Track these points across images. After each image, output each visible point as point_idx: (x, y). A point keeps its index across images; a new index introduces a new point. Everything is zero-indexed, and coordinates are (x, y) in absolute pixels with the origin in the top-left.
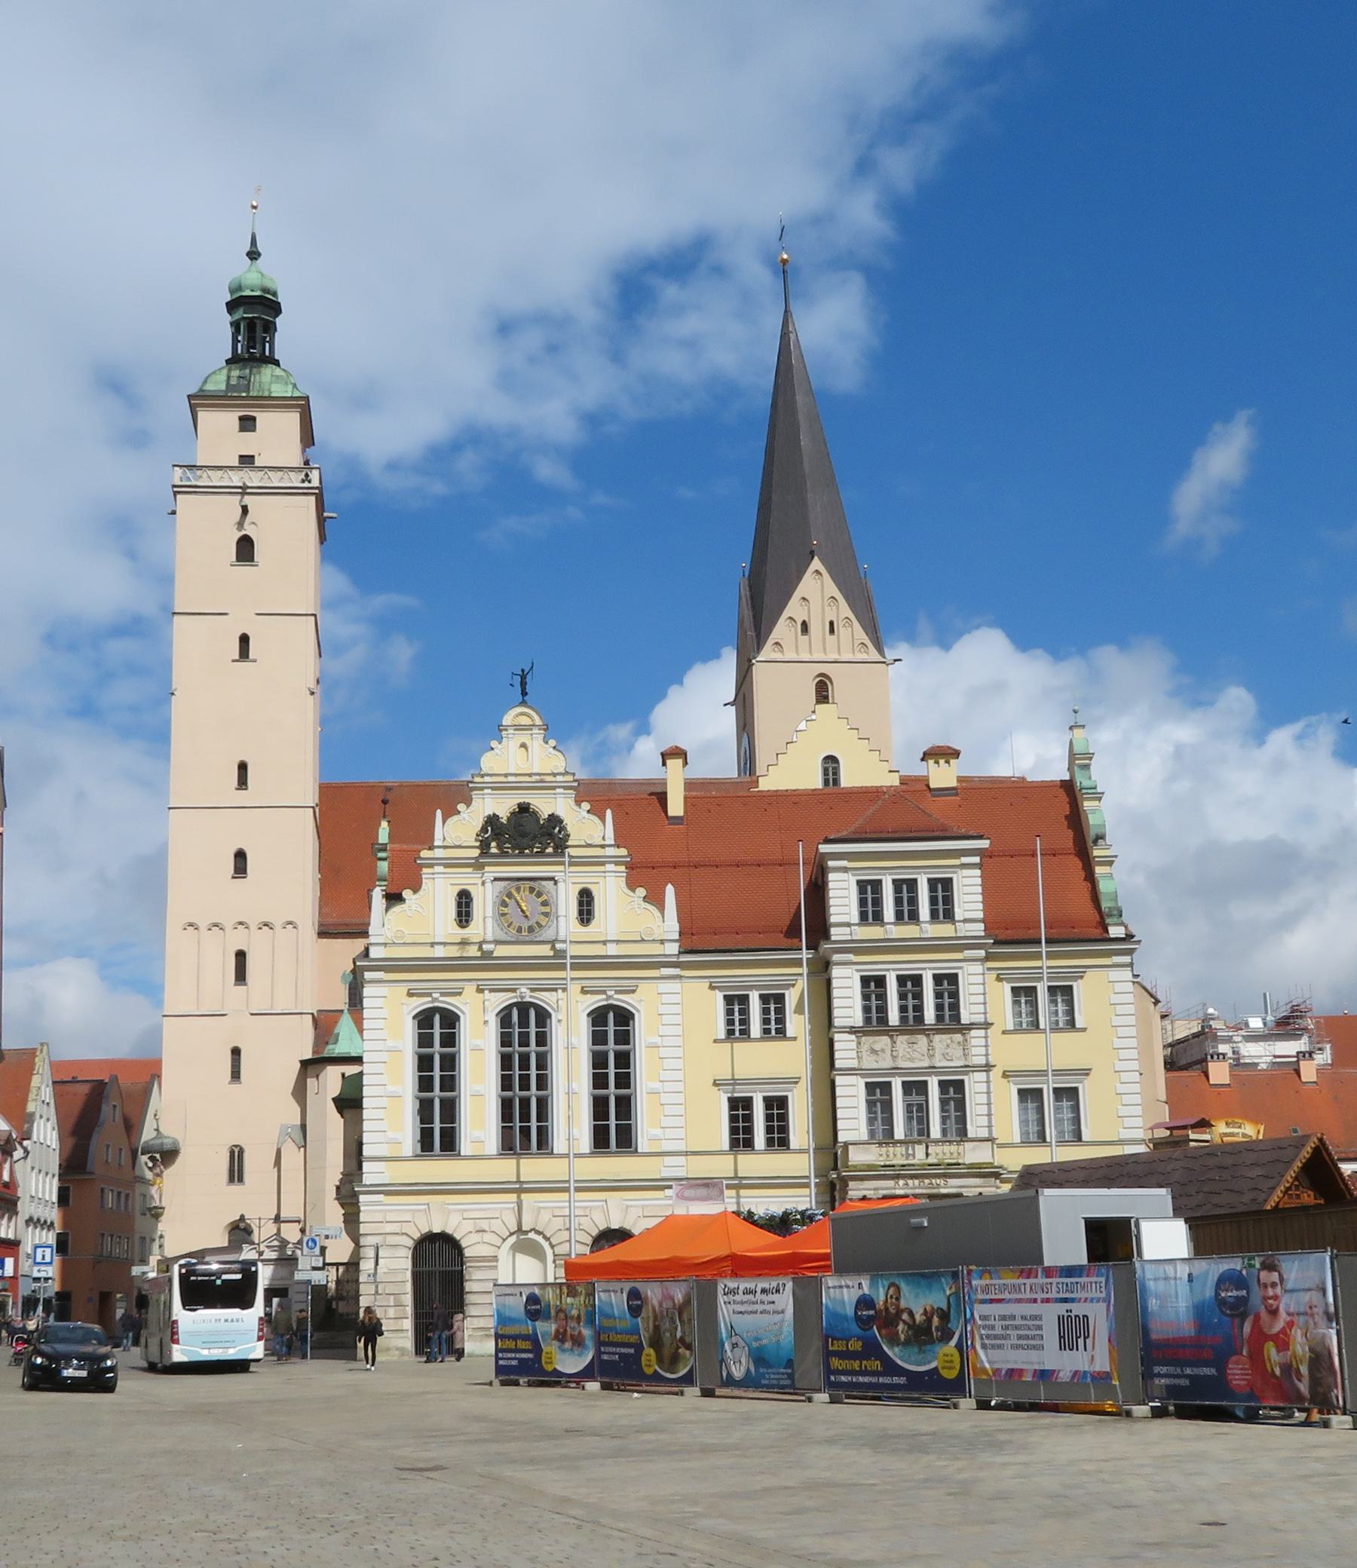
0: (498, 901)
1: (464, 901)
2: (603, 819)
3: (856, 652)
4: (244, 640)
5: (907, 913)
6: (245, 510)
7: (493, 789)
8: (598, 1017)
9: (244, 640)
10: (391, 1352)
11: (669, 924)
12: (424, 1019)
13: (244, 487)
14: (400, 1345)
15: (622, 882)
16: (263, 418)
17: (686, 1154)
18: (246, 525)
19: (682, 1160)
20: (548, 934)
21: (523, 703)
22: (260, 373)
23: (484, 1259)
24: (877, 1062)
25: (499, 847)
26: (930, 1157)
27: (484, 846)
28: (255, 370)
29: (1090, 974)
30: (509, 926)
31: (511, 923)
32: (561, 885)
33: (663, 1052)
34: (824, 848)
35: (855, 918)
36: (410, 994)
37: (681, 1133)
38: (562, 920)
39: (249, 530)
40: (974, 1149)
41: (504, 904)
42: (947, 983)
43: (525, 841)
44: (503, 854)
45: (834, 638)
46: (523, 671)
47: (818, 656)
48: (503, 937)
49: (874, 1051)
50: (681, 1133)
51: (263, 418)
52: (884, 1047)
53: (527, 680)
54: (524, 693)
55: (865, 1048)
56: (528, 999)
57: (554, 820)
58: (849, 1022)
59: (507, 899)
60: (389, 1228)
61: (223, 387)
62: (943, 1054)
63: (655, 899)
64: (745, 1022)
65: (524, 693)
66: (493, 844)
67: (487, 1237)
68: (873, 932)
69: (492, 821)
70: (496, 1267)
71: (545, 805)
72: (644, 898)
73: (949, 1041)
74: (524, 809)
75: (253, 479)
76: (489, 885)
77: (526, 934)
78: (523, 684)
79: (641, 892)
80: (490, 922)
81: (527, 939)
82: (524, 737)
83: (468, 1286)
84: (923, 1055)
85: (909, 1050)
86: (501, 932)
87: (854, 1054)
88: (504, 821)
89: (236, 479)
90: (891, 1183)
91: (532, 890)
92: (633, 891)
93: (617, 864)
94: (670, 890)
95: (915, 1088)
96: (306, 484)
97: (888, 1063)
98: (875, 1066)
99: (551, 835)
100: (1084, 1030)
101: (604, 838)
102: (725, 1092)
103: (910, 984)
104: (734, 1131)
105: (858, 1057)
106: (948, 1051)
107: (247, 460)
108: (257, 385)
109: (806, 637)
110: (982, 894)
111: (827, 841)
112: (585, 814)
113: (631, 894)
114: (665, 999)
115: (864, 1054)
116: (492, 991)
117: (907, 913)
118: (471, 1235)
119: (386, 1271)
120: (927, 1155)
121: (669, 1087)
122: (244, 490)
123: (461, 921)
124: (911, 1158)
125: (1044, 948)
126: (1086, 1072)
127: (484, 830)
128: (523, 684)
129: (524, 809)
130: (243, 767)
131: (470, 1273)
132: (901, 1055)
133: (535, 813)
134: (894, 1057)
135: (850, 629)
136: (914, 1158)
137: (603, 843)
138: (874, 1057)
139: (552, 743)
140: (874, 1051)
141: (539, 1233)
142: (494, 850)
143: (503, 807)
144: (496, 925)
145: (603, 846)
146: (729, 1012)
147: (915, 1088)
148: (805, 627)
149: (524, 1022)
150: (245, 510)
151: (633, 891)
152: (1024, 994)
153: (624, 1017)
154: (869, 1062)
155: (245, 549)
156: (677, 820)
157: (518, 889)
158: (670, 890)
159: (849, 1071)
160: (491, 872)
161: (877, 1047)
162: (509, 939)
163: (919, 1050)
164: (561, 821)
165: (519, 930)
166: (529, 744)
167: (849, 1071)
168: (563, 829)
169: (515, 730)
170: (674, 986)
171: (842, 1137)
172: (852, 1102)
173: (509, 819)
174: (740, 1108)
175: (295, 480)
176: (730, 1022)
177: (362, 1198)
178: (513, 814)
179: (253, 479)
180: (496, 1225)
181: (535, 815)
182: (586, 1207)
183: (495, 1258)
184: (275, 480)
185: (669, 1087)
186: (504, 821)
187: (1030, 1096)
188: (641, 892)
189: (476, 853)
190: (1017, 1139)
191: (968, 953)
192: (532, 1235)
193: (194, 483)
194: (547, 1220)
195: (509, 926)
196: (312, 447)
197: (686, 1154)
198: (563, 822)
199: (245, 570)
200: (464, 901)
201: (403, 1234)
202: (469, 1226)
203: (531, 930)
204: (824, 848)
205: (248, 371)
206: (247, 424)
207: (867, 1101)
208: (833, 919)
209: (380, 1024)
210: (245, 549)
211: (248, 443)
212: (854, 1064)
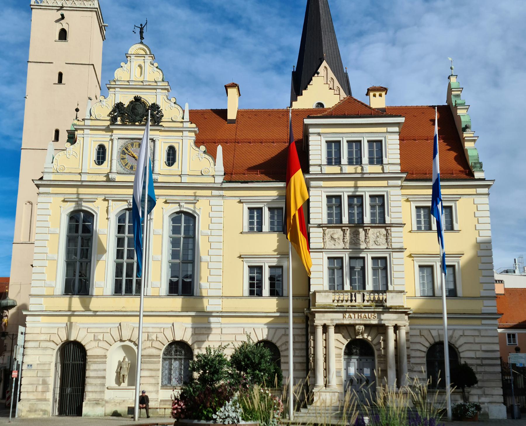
0: (120, 151)
4: (60, 75)
6: (63, 17)
7: (121, 88)
8: (176, 218)
9: (60, 75)
10: (38, 413)
11: (220, 168)
12: (74, 217)
14: (43, 409)
17: (222, 297)
19: (219, 301)
21: (141, 43)
23: (98, 357)
26: (366, 302)
27: (113, 120)
29: (463, 199)
30: (126, 165)
31: (127, 164)
34: (307, 121)
35: (324, 161)
36: (64, 201)
37: (220, 286)
39: (65, 27)
40: (392, 298)
41: (124, 153)
44: (124, 124)
46: (141, 25)
48: (121, 170)
50: (220, 286)
52: (339, 236)
53: (144, 30)
54: (142, 38)
55: (327, 237)
57: (155, 107)
60: (43, 337)
63: (212, 154)
64: (260, 223)
65: (142, 38)
66: (119, 119)
68: (335, 169)
69: (119, 107)
70: (105, 363)
71: (149, 98)
72: (204, 152)
73: (378, 234)
74: (137, 99)
78: (141, 33)
80: (115, 162)
83: (88, 373)
85: (354, 238)
86: (121, 168)
90: (340, 315)
92: (199, 148)
93: (190, 131)
94: (220, 149)
98: (333, 247)
101: (183, 118)
102: (247, 262)
104: (251, 285)
106: (378, 239)
110: (400, 159)
113: (197, 149)
116: (113, 200)
118: (91, 343)
119: (39, 363)
120: (364, 300)
123: (99, 162)
124: (354, 301)
127: (114, 111)
128: (141, 33)
129: (137, 99)
136: (356, 302)
137: (183, 120)
138: (333, 242)
139: (156, 65)
141: (130, 340)
142: (119, 123)
143: (126, 99)
144: (118, 164)
145: (182, 122)
146: (251, 217)
151: (199, 148)
153: (191, 217)
154: (330, 244)
155: (63, 35)
156: (232, 121)
157: (132, 145)
158: (220, 149)
160: (118, 133)
161: (335, 236)
162: (125, 172)
164: (159, 108)
166: (143, 65)
168: (160, 111)
169: (135, 56)
170: (220, 201)
171: (312, 290)
172: (320, 268)
176: (251, 223)
177: (28, 318)
178: (131, 102)
180: (108, 338)
181: (144, 104)
182: (161, 328)
183: (105, 357)
186: (125, 106)
188: (203, 148)
189: (108, 123)
191: (392, 183)
192: (128, 343)
193: (40, 4)
195: (126, 165)
197: (222, 297)
198: (159, 108)
199: (62, 43)
204: (307, 121)
207: (329, 268)
208: (311, 162)
210: (63, 35)
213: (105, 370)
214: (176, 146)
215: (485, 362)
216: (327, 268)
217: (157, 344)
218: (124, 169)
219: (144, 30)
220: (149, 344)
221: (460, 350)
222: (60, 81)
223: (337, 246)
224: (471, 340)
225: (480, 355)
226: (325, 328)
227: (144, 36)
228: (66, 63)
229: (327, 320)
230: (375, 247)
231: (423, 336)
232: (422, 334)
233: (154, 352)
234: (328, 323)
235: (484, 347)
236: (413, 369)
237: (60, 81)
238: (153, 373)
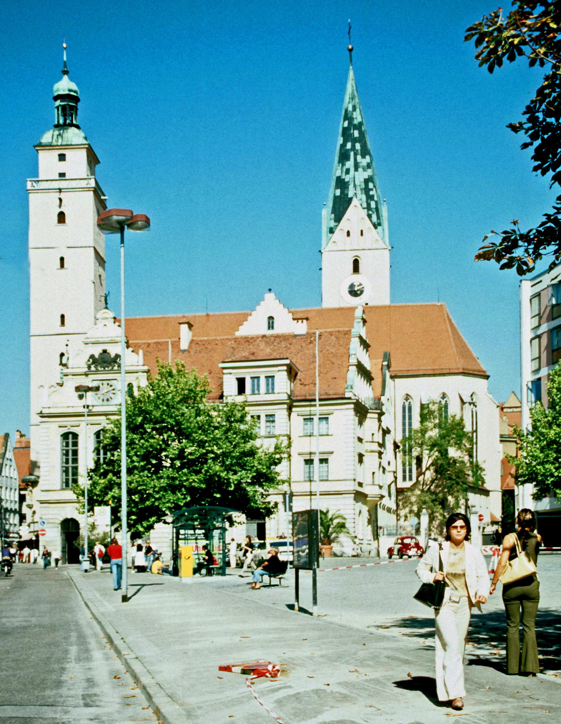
4: (62, 259)
6: (61, 200)
9: (62, 259)
16: (69, 153)
22: (67, 132)
25: (95, 367)
27: (89, 367)
28: (65, 131)
39: (63, 209)
43: (105, 365)
51: (69, 153)
54: (106, 303)
65: (106, 303)
69: (92, 357)
71: (113, 351)
74: (105, 351)
78: (106, 300)
82: (105, 322)
89: (57, 185)
91: (108, 384)
96: (89, 186)
99: (116, 362)
107: (62, 175)
111: (223, 362)
122: (60, 190)
125: (318, 403)
127: (89, 361)
128: (106, 300)
129: (105, 351)
130: (63, 317)
133: (109, 353)
137: (137, 364)
143: (97, 351)
150: (61, 200)
155: (61, 218)
156: (184, 351)
165: (103, 400)
173: (99, 356)
175: (83, 184)
178: (101, 354)
184: (74, 184)
193: (36, 188)
196: (99, 165)
199: (61, 226)
203: (108, 400)
205: (61, 132)
210: (61, 218)
211: (62, 167)
219: (108, 298)
222: (62, 266)
227: (108, 302)
237: (62, 266)
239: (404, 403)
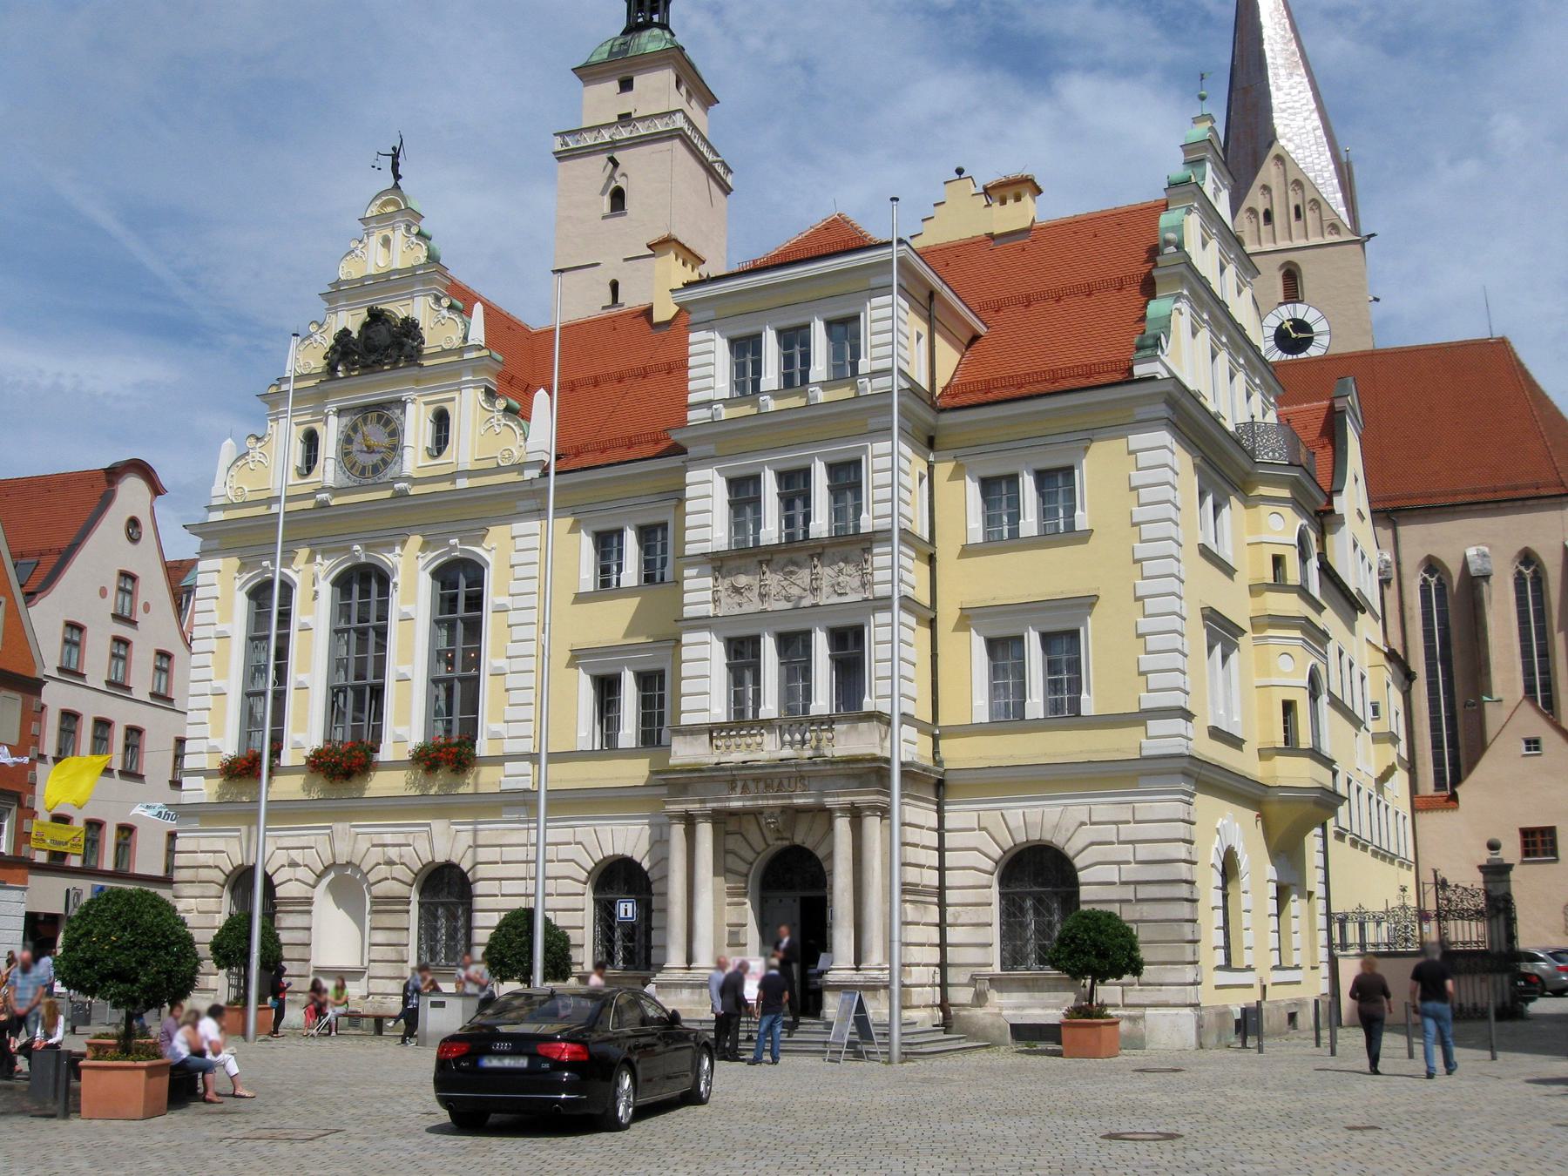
1: (311, 439)
2: (466, 312)
3: (1326, 235)
5: (795, 376)
6: (615, 164)
9: (615, 286)
13: (613, 142)
15: (480, 394)
18: (617, 175)
20: (392, 471)
22: (639, 37)
24: (740, 605)
25: (348, 370)
27: (331, 369)
30: (352, 468)
32: (409, 407)
33: (513, 617)
38: (408, 454)
39: (621, 182)
42: (846, 478)
45: (1301, 223)
46: (394, 149)
47: (1282, 244)
48: (346, 482)
49: (737, 590)
54: (397, 177)
56: (363, 559)
57: (410, 328)
58: (708, 548)
59: (352, 434)
61: (605, 56)
62: (833, 586)
65: (397, 177)
66: (340, 368)
67: (301, 872)
70: (309, 912)
71: (399, 309)
74: (376, 317)
75: (624, 133)
76: (333, 420)
77: (370, 475)
78: (395, 166)
79: (501, 404)
81: (370, 481)
84: (806, 590)
85: (785, 583)
87: (708, 595)
88: (355, 335)
89: (606, 136)
91: (380, 418)
95: (794, 645)
97: (754, 605)
100: (1086, 536)
101: (465, 338)
103: (795, 485)
105: (715, 601)
106: (841, 579)
107: (625, 118)
108: (635, 47)
109: (1270, 227)
112: (445, 312)
114: (520, 543)
115: (723, 595)
117: (795, 376)
121: (518, 664)
122: (614, 145)
126: (1087, 603)
128: (395, 166)
129: (376, 317)
131: (279, 919)
132: (773, 592)
134: (762, 596)
135: (1317, 211)
138: (737, 599)
140: (737, 590)
145: (460, 351)
147: (794, 645)
148: (1268, 216)
149: (365, 593)
151: (493, 405)
152: (998, 490)
153: (473, 571)
154: (729, 607)
159: (701, 623)
162: (350, 484)
163: (798, 582)
167: (701, 623)
174: (607, 688)
179: (624, 133)
183: (308, 901)
185: (518, 664)
186: (355, 335)
187: (1003, 650)
188: (501, 404)
190: (982, 716)
194: (365, 850)
195: (352, 468)
199: (617, 221)
200: (311, 439)
201: (216, 867)
202: (282, 857)
203: (376, 469)
205: (630, 37)
206: (626, 85)
209: (213, 604)
212: (709, 610)
213: (309, 929)
214: (447, 406)
215: (1144, 892)
216: (725, 669)
217: (398, 871)
218: (348, 477)
220: (384, 870)
221: (1078, 862)
223: (747, 608)
224: (1109, 832)
225: (1132, 872)
226: (690, 821)
228: (626, 260)
229: (693, 802)
230: (835, 599)
231: (985, 829)
232: (982, 825)
233: (397, 889)
234: (693, 807)
235: (1144, 852)
236: (956, 919)
238: (393, 937)
239: (1425, 580)
